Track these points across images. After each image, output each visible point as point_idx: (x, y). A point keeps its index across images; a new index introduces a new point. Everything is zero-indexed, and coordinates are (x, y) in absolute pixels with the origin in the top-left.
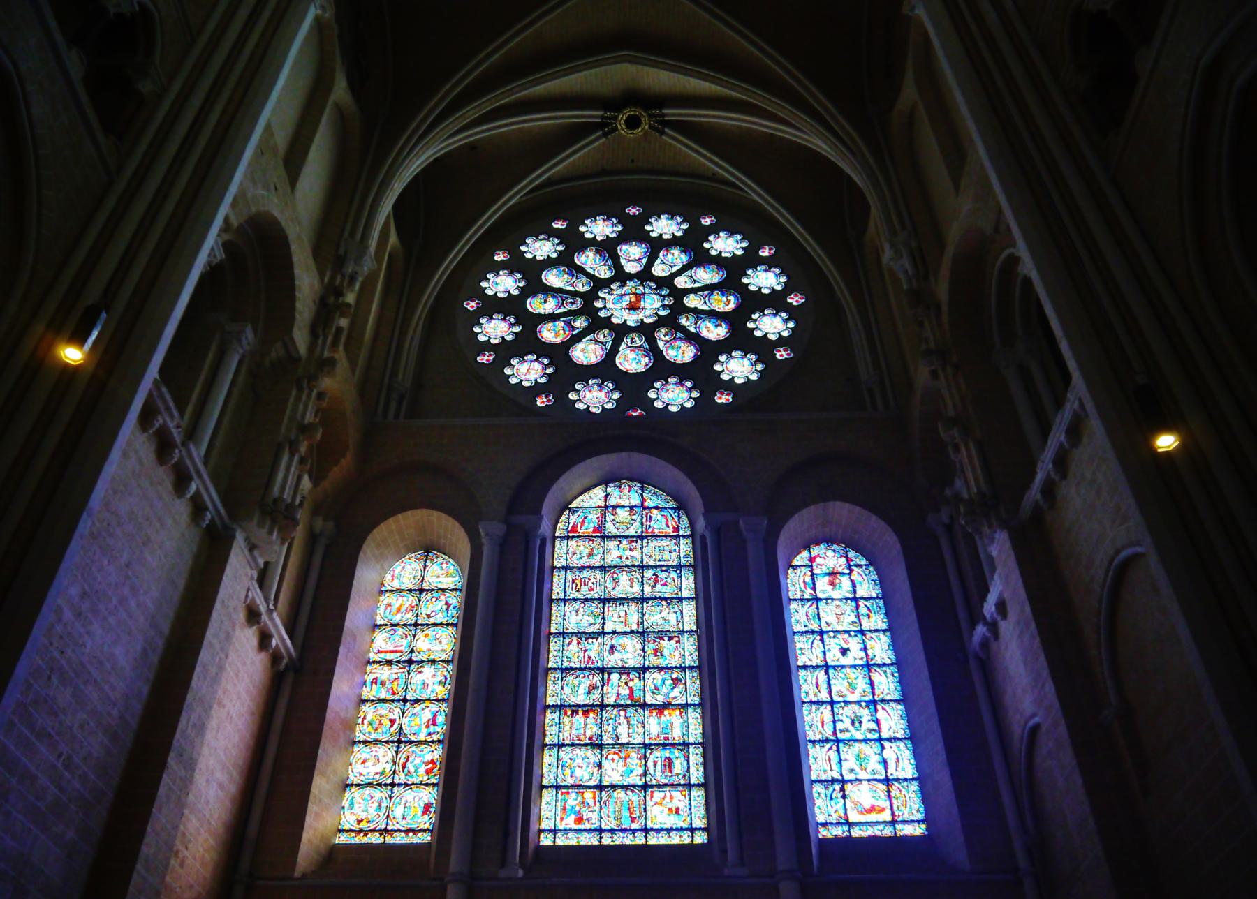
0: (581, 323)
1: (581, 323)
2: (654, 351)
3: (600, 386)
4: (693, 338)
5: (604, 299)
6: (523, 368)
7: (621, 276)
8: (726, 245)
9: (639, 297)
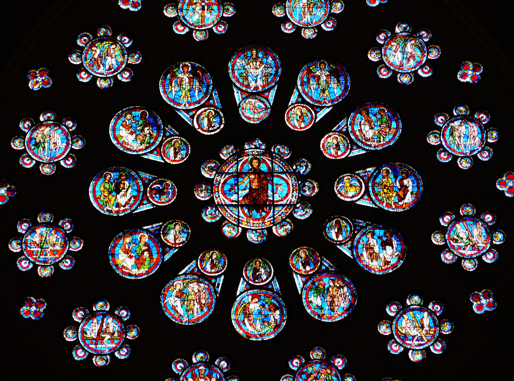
0: (175, 235)
1: (175, 235)
2: (290, 299)
3: (209, 364)
4: (348, 269)
5: (210, 182)
6: (92, 329)
7: (237, 132)
8: (403, 56)
9: (265, 178)
